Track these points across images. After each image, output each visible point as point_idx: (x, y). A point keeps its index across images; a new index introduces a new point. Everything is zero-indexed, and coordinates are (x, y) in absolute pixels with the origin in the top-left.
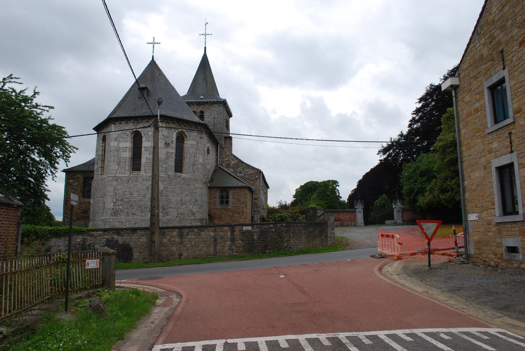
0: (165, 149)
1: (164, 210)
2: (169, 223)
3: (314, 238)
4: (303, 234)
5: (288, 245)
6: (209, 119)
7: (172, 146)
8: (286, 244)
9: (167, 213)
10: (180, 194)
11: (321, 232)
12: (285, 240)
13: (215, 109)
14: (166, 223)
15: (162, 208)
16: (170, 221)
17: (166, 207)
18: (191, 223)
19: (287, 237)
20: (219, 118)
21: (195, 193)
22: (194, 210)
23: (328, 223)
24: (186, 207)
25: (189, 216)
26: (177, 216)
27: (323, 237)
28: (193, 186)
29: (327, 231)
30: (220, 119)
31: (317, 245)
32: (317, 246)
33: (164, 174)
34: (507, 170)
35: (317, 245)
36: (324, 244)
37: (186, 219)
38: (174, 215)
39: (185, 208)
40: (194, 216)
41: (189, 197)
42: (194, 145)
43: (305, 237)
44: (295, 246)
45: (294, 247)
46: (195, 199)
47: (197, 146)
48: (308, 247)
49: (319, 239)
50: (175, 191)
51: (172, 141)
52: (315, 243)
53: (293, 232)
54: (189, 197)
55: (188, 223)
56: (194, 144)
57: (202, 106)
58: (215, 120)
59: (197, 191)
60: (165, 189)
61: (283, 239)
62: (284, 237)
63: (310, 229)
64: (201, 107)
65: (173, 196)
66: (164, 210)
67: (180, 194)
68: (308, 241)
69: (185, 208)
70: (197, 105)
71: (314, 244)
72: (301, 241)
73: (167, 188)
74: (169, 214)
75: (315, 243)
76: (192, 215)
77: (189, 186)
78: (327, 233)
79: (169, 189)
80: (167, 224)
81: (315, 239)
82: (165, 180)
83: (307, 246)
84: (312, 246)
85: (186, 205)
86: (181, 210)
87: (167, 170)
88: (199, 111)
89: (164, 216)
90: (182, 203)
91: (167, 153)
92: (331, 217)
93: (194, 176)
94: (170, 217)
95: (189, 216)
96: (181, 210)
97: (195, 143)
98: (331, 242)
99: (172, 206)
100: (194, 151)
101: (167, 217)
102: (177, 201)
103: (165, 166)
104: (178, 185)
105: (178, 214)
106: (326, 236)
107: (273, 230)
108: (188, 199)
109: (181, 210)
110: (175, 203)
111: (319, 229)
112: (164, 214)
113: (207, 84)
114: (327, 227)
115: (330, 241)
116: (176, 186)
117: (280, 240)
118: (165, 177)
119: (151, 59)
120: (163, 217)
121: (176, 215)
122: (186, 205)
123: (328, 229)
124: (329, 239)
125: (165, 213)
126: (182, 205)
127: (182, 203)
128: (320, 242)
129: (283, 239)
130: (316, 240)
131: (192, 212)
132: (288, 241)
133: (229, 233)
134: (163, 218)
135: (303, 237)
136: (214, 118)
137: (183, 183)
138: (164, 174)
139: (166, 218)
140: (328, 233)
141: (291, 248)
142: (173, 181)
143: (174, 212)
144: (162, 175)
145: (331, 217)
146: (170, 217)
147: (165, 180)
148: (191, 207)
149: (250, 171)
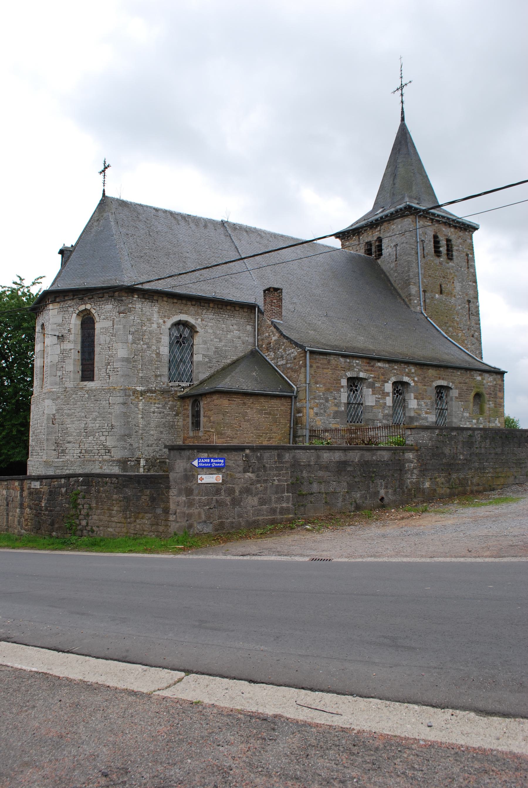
0: (58, 346)
1: (58, 446)
2: (66, 468)
3: (139, 513)
4: (114, 502)
5: (87, 523)
6: (390, 249)
7: (70, 339)
8: (84, 523)
9: (63, 451)
10: (83, 417)
11: (153, 499)
12: (82, 512)
13: (397, 226)
14: (61, 468)
15: (56, 443)
16: (66, 465)
17: (61, 442)
18: (101, 468)
19: (85, 506)
20: (403, 243)
21: (110, 413)
22: (108, 444)
23: (171, 479)
24: (94, 439)
25: (100, 454)
26: (79, 457)
27: (159, 511)
28: (104, 402)
29: (168, 498)
30: (404, 245)
31: (144, 531)
32: (145, 533)
33: (58, 387)
34: (471, 248)
35: (144, 531)
36: (161, 529)
37: (93, 461)
38: (75, 455)
39: (93, 442)
40: (109, 454)
41: (98, 422)
42: (107, 329)
43: (119, 509)
44: (101, 528)
45: (100, 530)
46: (110, 425)
47: (113, 329)
48: (127, 533)
49: (150, 515)
50: (74, 413)
51: (69, 331)
52: (140, 524)
53: (96, 498)
54: (98, 421)
55: (97, 467)
56: (107, 326)
57: (379, 228)
58: (398, 248)
59: (112, 411)
60: (58, 413)
61: (78, 510)
62: (81, 507)
63: (129, 492)
64: (377, 230)
65: (73, 422)
66: (58, 446)
67: (83, 417)
68: (126, 518)
69: (93, 442)
70: (371, 228)
71: (138, 526)
72: (113, 519)
73: (62, 409)
74: (67, 452)
75: (140, 524)
76: (106, 453)
77: (99, 402)
78: (168, 502)
79: (65, 411)
80: (62, 469)
81: (141, 516)
82: (59, 397)
83: (124, 530)
84: (133, 532)
85: (94, 436)
86: (87, 445)
87: (64, 379)
88: (375, 239)
89: (60, 457)
90: (88, 432)
91: (63, 352)
92: (178, 461)
93: (109, 383)
94: (68, 457)
95: (100, 454)
96: (86, 446)
97: (110, 323)
98: (178, 525)
99: (70, 439)
100: (108, 339)
101: (64, 457)
102: (78, 431)
103: (59, 373)
104: (79, 403)
105: (80, 453)
106: (166, 511)
107: (63, 490)
108: (98, 425)
109: (87, 445)
110: (75, 434)
111: (148, 492)
112: (59, 453)
113: (396, 181)
114: (168, 488)
115: (174, 523)
116: (76, 404)
117: (72, 512)
118: (58, 393)
119: (100, 197)
120: (58, 458)
121: (78, 455)
122: (94, 436)
123: (171, 494)
124: (172, 518)
125: (60, 451)
126: (87, 436)
127: (88, 432)
128: (152, 525)
129: (78, 510)
130: (142, 518)
131: (105, 448)
132: (88, 515)
133: (19, 492)
134: (56, 460)
135: (115, 508)
136: (396, 245)
137: (88, 398)
138: (58, 387)
139: (61, 460)
140: (171, 501)
141: (93, 531)
142: (70, 397)
143: (74, 450)
144: (55, 390)
145: (178, 461)
146: (68, 457)
147: (59, 397)
148: (103, 438)
149: (293, 353)
